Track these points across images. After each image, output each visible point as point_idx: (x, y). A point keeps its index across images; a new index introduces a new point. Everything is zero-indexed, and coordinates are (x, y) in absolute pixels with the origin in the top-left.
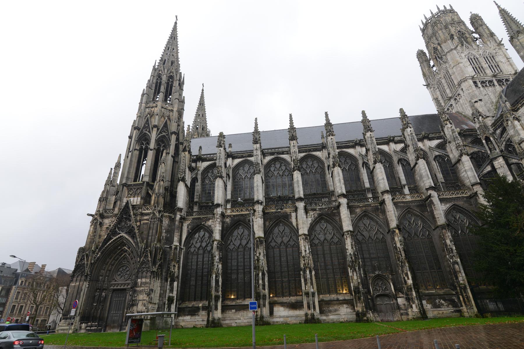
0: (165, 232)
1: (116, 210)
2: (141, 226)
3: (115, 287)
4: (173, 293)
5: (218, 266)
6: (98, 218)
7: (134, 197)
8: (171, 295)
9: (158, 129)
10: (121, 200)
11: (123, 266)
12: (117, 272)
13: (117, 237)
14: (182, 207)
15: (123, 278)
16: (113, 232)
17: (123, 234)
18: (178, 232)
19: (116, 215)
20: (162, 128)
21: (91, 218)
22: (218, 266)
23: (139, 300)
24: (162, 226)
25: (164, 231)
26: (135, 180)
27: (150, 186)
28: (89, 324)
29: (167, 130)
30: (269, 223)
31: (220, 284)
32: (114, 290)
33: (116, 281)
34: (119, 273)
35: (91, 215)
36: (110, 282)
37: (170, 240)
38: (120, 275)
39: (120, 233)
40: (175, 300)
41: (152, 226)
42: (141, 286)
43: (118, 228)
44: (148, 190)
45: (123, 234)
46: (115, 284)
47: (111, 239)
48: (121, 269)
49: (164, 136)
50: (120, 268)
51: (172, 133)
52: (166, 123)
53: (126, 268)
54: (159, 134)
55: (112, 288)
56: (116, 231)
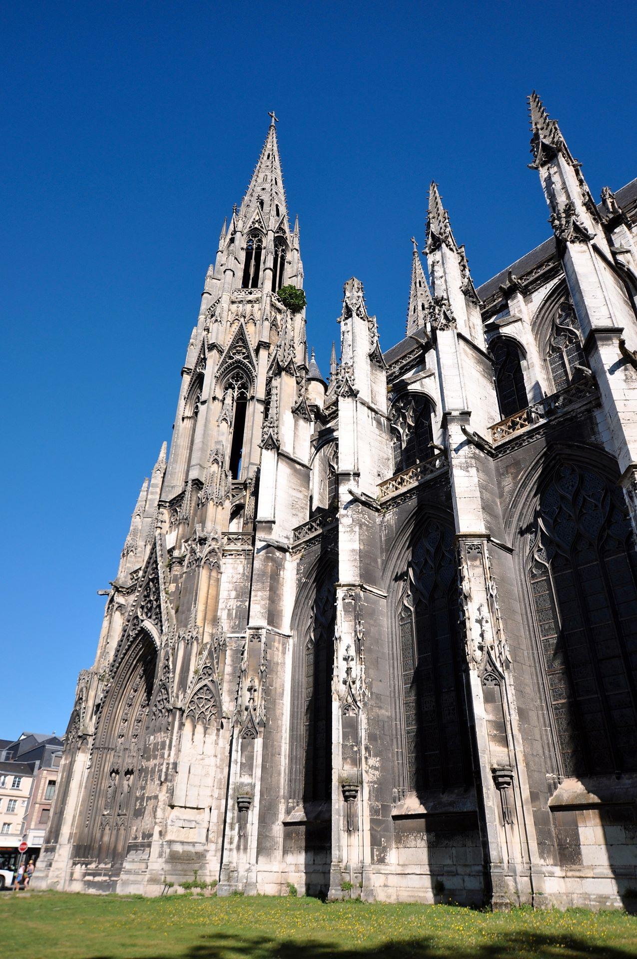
0: (237, 597)
5: (349, 670)
9: (221, 352)
14: (271, 518)
18: (263, 589)
20: (232, 347)
22: (349, 670)
24: (218, 581)
25: (233, 594)
29: (246, 346)
30: (514, 478)
31: (363, 734)
49: (239, 361)
51: (257, 351)
54: (224, 362)
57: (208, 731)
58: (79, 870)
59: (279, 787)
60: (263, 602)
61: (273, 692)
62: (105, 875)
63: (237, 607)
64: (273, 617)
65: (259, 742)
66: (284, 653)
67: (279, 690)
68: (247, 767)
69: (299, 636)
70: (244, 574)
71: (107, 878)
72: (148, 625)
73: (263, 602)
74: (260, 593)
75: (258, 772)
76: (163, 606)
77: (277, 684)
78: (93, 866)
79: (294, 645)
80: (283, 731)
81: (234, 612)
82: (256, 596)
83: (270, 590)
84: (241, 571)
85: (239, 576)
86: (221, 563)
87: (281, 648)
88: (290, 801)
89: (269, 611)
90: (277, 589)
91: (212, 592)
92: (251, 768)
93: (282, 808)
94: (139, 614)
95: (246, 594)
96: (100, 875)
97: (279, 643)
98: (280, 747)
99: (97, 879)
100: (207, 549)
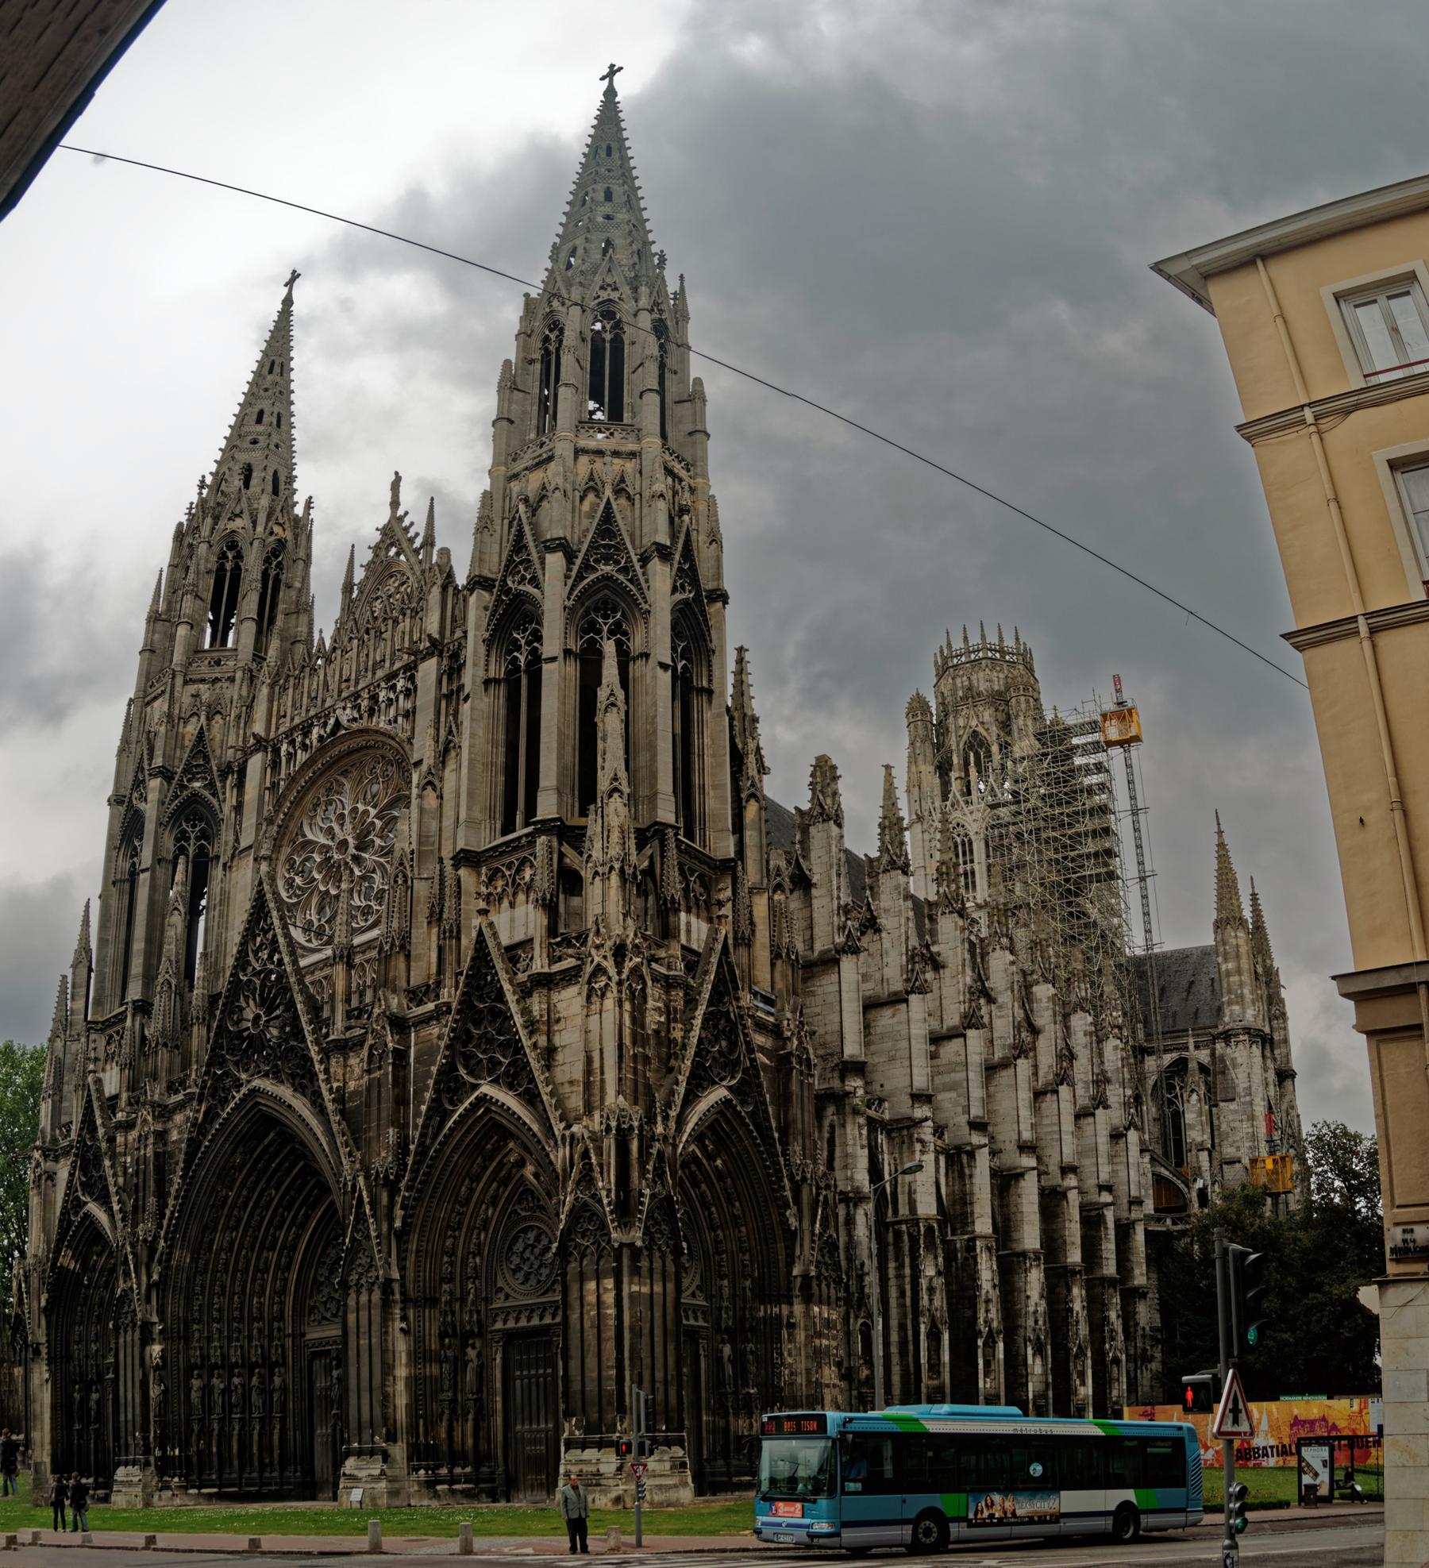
1: (449, 980)
3: (511, 1324)
7: (512, 905)
10: (455, 933)
11: (525, 1230)
12: (508, 1260)
13: (466, 1104)
15: (533, 1281)
17: (487, 1089)
26: (508, 827)
27: (572, 836)
28: (444, 1471)
32: (509, 1337)
33: (507, 1296)
34: (516, 1260)
36: (488, 1300)
38: (518, 1269)
39: (475, 1087)
43: (467, 1058)
44: (561, 855)
45: (487, 1089)
46: (506, 1312)
47: (445, 1115)
48: (519, 1246)
50: (516, 1239)
52: (608, 516)
53: (538, 1239)
55: (499, 1325)
56: (458, 1078)
94: (462, 1072)
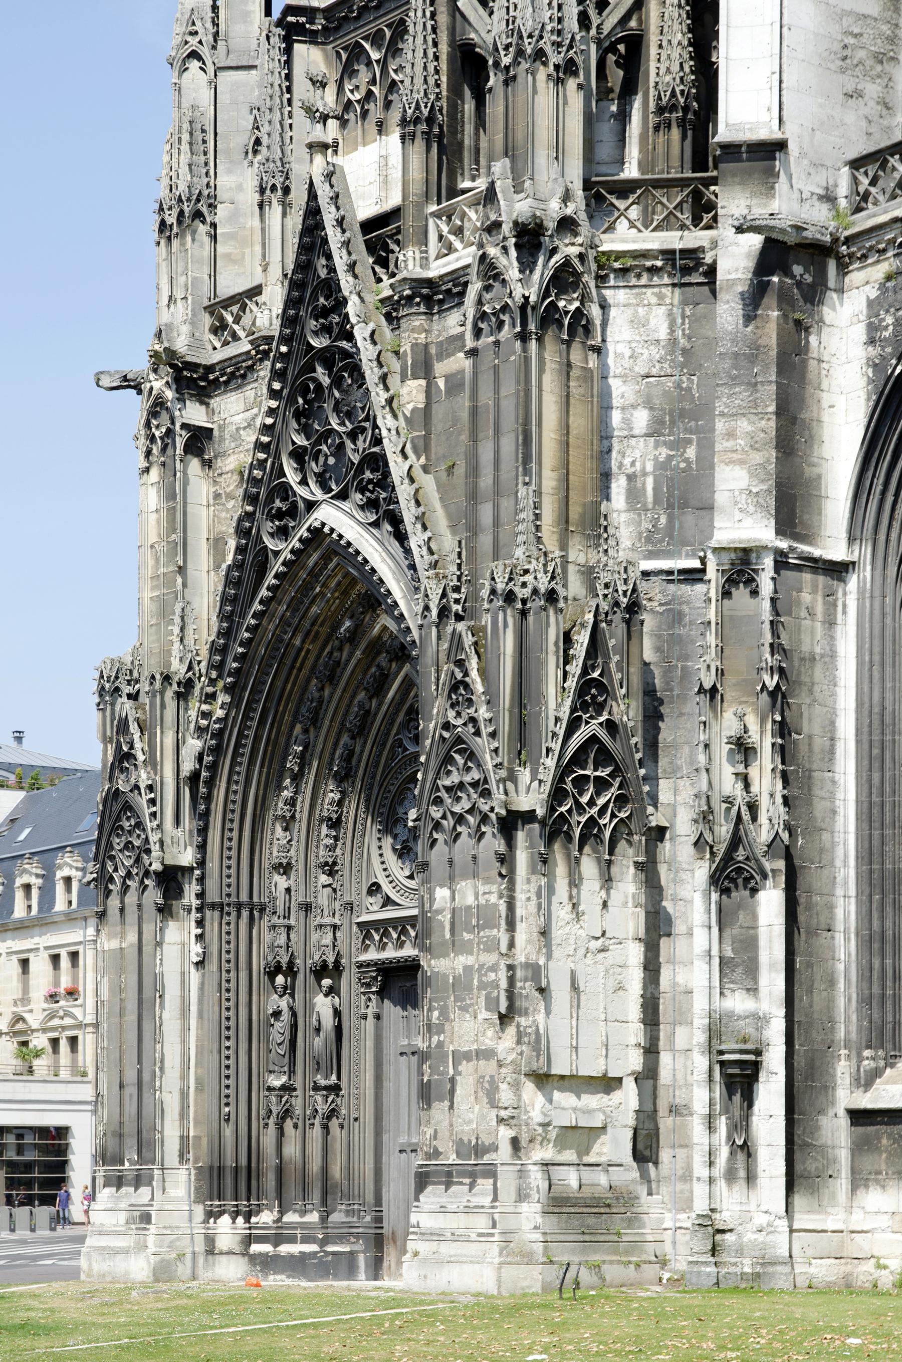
0: (654, 431)
2: (438, 412)
4: (753, 990)
6: (169, 394)
8: (738, 1002)
16: (269, 500)
18: (753, 409)
19: (262, 346)
21: (134, 407)
23: (459, 1057)
25: (641, 419)
35: (130, 383)
37: (685, 497)
40: (774, 1060)
41: (486, 397)
42: (456, 946)
57: (614, 870)
58: (227, 1230)
59: (832, 1020)
60: (757, 458)
61: (803, 749)
62: (305, 1240)
63: (662, 466)
64: (791, 504)
65: (770, 903)
66: (830, 623)
67: (819, 742)
68: (737, 966)
69: (880, 560)
70: (673, 342)
71: (314, 1248)
72: (341, 519)
73: (757, 458)
74: (744, 425)
75: (772, 981)
76: (397, 468)
77: (810, 725)
78: (266, 1217)
79: (861, 591)
80: (838, 863)
81: (650, 482)
82: (730, 435)
83: (779, 413)
84: (663, 333)
85: (656, 353)
86: (595, 311)
87: (819, 608)
88: (867, 1053)
89: (779, 485)
90: (802, 402)
91: (579, 422)
92: (752, 970)
93: (843, 1070)
94: (292, 477)
95: (681, 417)
96: (292, 1240)
97: (814, 591)
98: (831, 907)
99: (285, 1249)
100: (542, 271)
